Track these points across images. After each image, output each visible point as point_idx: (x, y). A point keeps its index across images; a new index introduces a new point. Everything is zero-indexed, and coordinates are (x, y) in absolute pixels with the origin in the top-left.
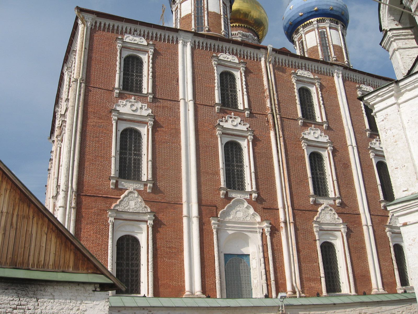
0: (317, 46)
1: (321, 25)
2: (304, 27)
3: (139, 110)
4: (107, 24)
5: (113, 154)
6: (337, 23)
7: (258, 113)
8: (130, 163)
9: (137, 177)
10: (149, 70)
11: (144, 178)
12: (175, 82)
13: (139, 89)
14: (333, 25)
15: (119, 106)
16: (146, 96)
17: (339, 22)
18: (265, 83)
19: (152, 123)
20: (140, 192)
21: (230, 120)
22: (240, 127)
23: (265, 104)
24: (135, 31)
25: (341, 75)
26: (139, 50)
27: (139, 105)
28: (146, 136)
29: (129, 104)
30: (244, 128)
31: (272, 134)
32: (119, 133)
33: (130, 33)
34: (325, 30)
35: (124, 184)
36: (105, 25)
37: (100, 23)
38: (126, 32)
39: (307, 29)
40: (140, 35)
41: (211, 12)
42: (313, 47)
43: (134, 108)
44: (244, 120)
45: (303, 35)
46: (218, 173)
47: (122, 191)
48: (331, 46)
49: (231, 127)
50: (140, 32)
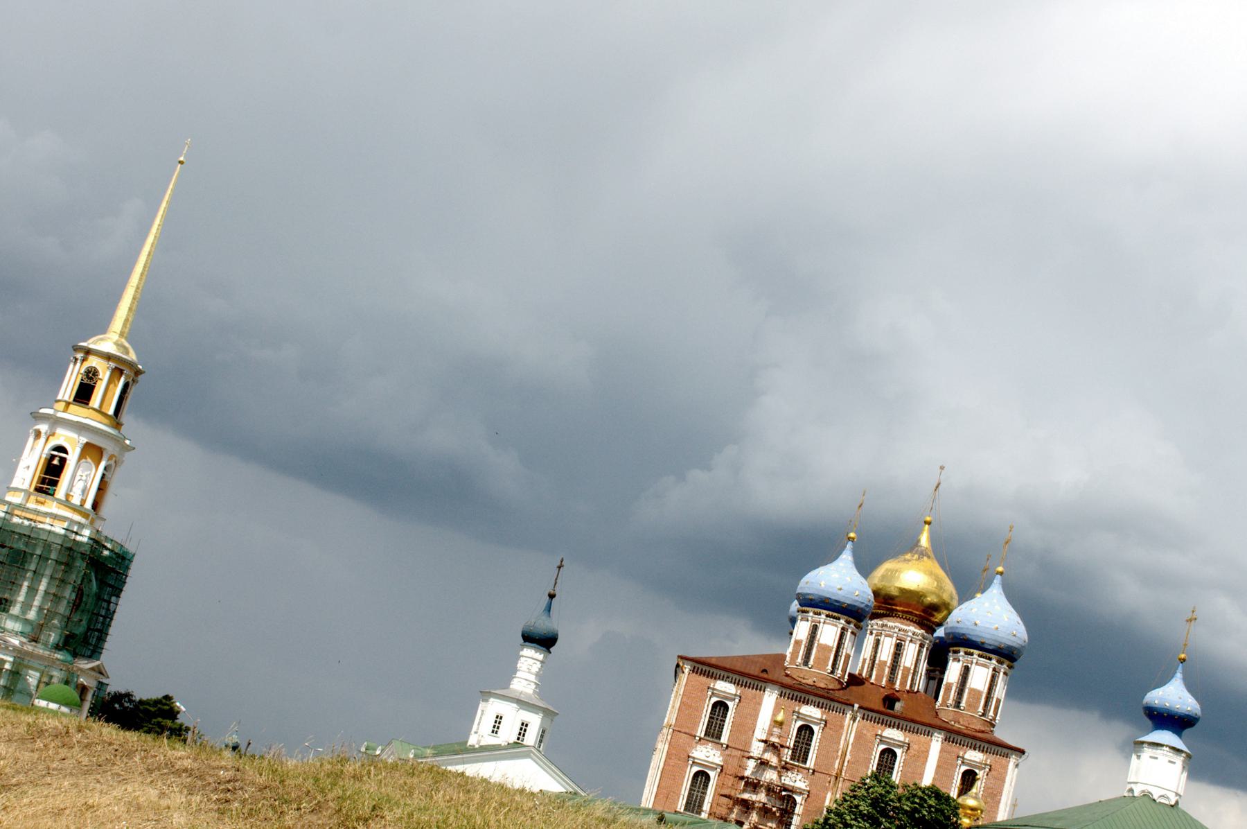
4: (704, 669)
6: (990, 659)
7: (824, 772)
8: (696, 799)
12: (751, 733)
15: (696, 751)
17: (991, 656)
18: (842, 742)
23: (833, 763)
24: (728, 677)
27: (714, 752)
29: (705, 750)
33: (723, 680)
34: (969, 665)
36: (702, 670)
37: (698, 668)
38: (719, 678)
40: (731, 682)
41: (821, 644)
43: (708, 754)
50: (732, 679)
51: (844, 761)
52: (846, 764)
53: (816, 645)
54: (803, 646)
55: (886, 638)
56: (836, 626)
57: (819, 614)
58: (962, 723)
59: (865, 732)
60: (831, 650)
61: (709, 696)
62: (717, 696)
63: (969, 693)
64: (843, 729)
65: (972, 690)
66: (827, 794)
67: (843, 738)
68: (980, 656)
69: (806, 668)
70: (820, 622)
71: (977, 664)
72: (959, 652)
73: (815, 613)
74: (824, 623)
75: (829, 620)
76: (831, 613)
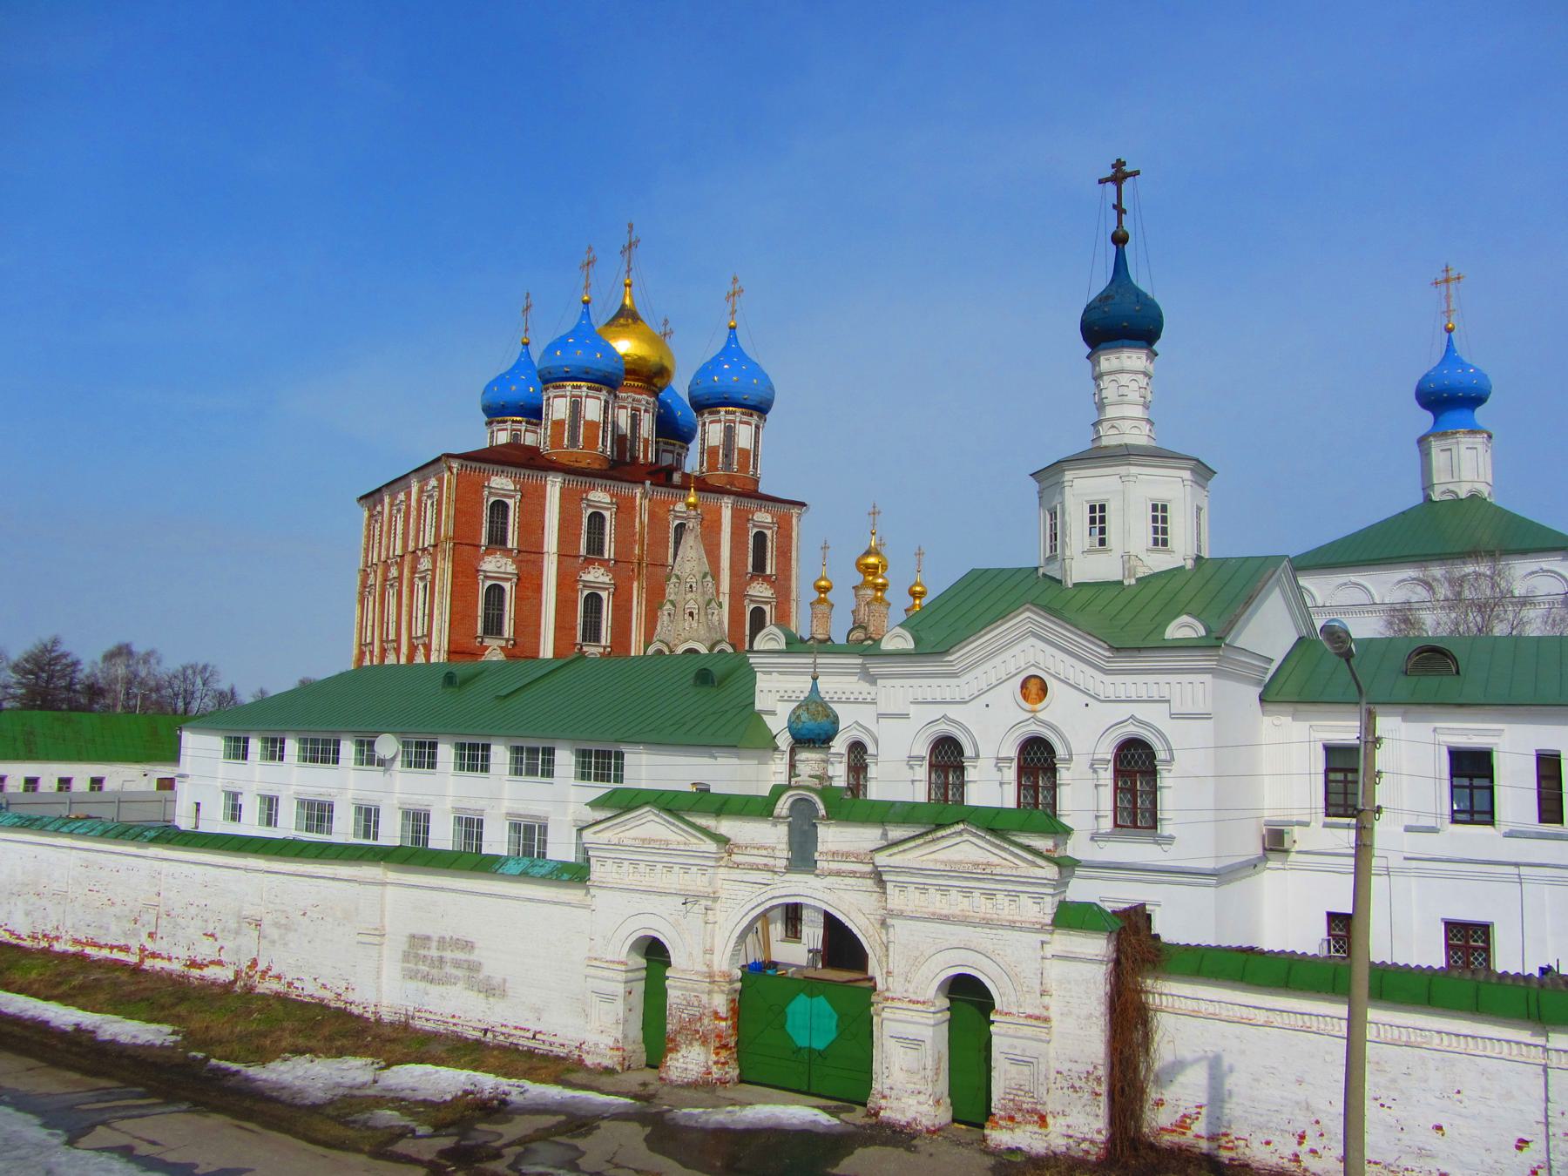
1: (730, 417)
2: (710, 413)
3: (503, 567)
4: (474, 466)
5: (479, 614)
9: (499, 632)
10: (514, 520)
11: (506, 636)
13: (504, 541)
14: (745, 418)
16: (512, 550)
17: (754, 412)
18: (637, 525)
19: (515, 580)
20: (501, 648)
21: (592, 571)
22: (602, 579)
23: (633, 549)
24: (502, 472)
25: (730, 505)
26: (506, 496)
27: (505, 560)
28: (509, 593)
30: (606, 579)
31: (635, 585)
32: (485, 590)
34: (733, 425)
35: (487, 642)
38: (492, 475)
41: (588, 421)
42: (714, 447)
43: (499, 564)
44: (609, 570)
45: (707, 424)
46: (574, 628)
47: (487, 648)
48: (736, 450)
49: (592, 579)
51: (643, 545)
52: (645, 548)
53: (582, 422)
54: (567, 426)
55: (620, 410)
56: (599, 398)
57: (580, 387)
58: (737, 485)
59: (657, 510)
60: (599, 427)
61: (486, 497)
62: (496, 495)
63: (739, 454)
64: (635, 510)
65: (741, 450)
66: (633, 583)
67: (637, 520)
68: (743, 414)
69: (575, 450)
70: (581, 397)
71: (741, 422)
72: (719, 412)
74: (587, 396)
75: (591, 393)
76: (593, 385)
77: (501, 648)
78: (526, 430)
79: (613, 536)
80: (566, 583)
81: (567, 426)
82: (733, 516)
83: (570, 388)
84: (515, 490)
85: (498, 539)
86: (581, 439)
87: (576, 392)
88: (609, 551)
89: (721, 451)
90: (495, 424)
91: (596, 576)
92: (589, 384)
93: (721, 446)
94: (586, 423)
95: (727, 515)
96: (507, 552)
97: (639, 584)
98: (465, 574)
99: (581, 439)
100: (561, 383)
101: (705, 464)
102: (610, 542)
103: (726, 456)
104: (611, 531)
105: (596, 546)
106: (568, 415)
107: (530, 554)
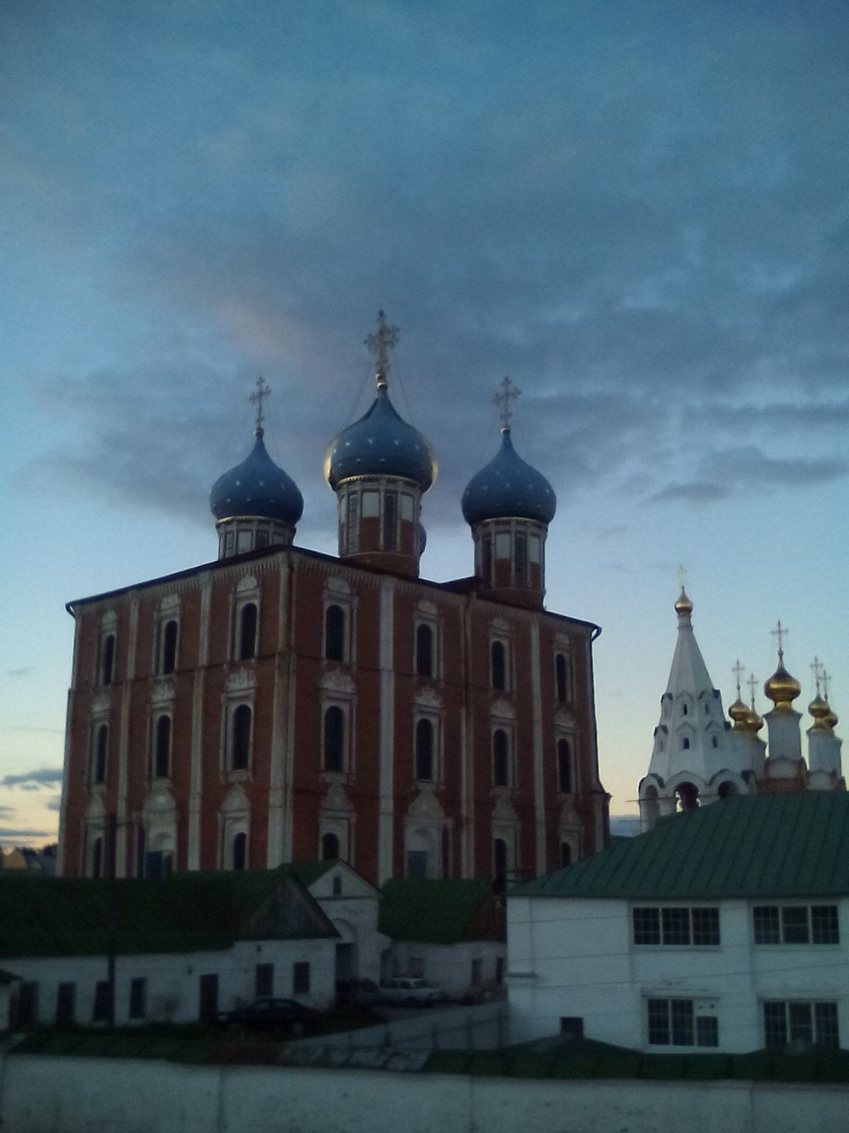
0: (510, 559)
2: (497, 523)
31: (463, 711)
33: (334, 576)
34: (523, 537)
35: (328, 777)
39: (501, 528)
45: (493, 535)
54: (382, 525)
73: (389, 481)
75: (408, 490)
77: (343, 785)
78: (275, 533)
79: (441, 653)
80: (404, 707)
81: (382, 525)
82: (542, 637)
83: (383, 482)
84: (351, 595)
85: (335, 652)
86: (398, 541)
87: (392, 487)
88: (438, 669)
89: (513, 565)
90: (235, 523)
91: (428, 700)
92: (407, 479)
93: (513, 559)
94: (402, 520)
95: (535, 634)
96: (347, 669)
97: (467, 710)
98: (309, 693)
99: (398, 541)
100: (374, 476)
101: (493, 578)
102: (439, 659)
103: (518, 570)
104: (438, 646)
105: (425, 668)
106: (382, 513)
107: (367, 672)
